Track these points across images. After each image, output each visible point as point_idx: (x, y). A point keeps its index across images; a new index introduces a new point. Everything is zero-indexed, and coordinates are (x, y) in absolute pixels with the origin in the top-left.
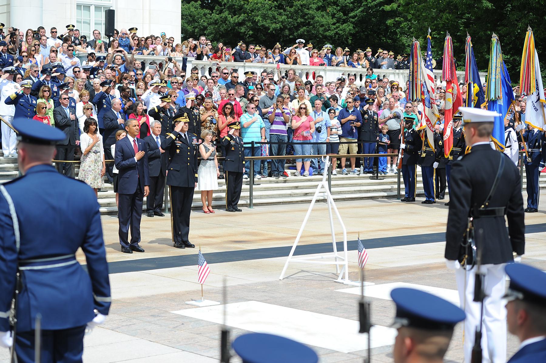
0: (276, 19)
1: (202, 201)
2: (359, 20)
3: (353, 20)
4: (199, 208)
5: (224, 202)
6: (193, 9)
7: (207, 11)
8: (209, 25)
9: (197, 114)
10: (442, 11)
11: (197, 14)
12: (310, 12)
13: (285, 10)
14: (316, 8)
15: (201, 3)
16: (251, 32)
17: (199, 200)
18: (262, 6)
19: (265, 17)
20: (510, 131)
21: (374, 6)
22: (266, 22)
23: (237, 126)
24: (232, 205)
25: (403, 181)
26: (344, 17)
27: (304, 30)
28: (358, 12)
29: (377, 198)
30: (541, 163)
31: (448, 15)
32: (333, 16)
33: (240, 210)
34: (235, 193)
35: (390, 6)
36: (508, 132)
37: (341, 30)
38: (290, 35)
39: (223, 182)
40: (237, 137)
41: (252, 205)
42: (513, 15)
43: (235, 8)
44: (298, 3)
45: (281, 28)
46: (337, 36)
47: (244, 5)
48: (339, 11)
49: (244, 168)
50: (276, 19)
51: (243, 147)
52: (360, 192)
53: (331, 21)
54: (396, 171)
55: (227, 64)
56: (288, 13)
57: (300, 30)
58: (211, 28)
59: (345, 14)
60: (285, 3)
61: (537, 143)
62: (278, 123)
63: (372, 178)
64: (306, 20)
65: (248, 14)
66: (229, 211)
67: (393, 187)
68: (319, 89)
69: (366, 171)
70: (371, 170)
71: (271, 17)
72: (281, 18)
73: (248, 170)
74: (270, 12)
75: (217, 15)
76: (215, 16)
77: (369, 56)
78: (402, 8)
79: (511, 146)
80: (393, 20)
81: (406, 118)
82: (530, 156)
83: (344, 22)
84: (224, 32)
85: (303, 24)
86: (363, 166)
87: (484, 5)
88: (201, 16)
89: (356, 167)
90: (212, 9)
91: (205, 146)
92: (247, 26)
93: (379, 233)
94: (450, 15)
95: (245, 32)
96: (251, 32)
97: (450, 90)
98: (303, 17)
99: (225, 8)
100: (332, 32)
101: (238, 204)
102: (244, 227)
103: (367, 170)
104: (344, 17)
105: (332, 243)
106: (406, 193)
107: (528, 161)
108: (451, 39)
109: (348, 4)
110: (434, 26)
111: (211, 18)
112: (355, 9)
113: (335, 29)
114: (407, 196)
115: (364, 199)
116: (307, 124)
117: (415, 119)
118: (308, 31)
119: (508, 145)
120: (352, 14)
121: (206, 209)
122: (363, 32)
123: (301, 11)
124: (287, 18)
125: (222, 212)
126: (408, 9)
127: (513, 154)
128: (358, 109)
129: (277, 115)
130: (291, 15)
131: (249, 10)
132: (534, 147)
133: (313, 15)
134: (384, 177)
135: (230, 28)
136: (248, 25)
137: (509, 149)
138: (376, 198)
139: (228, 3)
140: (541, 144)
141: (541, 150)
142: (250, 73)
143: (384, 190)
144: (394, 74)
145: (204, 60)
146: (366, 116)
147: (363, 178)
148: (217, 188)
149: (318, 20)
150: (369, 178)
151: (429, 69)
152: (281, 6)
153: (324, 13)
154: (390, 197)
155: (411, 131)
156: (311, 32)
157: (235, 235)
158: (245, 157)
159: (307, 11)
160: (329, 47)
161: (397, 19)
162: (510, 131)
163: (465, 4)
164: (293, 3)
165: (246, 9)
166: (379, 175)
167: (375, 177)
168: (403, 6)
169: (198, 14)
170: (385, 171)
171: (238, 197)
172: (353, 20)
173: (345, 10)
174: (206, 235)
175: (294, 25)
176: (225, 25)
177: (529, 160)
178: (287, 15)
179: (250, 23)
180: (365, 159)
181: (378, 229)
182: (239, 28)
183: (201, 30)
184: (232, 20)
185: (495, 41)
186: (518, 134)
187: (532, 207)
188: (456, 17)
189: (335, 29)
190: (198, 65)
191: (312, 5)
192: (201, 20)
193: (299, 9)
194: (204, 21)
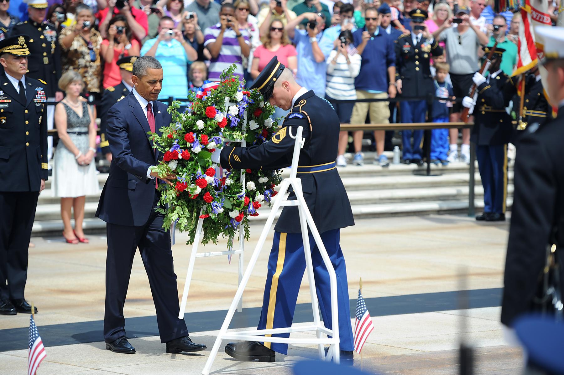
1: (63, 218)
62: (226, 59)
63: (417, 173)
69: (409, 159)
70: (417, 156)
81: (487, 49)
86: (400, 149)
105: (311, 304)
106: (486, 203)
115: (400, 215)
134: (442, 172)
166: (432, 166)
167: (423, 170)
180: (404, 134)
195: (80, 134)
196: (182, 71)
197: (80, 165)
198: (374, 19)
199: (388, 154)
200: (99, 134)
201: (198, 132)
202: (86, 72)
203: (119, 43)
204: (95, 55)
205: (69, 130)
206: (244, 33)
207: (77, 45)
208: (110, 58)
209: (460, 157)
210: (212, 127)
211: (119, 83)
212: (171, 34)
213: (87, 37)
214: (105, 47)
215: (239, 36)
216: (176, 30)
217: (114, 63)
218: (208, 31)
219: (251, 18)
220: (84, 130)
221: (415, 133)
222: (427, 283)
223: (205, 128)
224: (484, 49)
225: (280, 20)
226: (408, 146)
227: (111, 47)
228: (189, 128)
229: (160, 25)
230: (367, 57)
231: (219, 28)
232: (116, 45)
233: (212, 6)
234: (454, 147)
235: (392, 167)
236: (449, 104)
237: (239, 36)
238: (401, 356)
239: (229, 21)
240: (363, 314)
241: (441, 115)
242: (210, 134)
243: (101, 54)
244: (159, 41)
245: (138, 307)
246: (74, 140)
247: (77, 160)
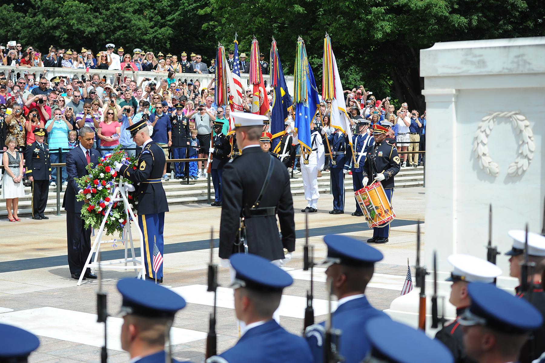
0: (91, 23)
1: (7, 210)
2: (177, 23)
3: (171, 23)
4: (5, 217)
5: (30, 210)
6: (5, 12)
7: (20, 14)
8: (23, 28)
9: (2, 121)
10: (255, 15)
11: (10, 17)
12: (127, 15)
13: (101, 14)
14: (132, 12)
15: (13, 6)
16: (66, 36)
17: (4, 209)
18: (77, 9)
19: (80, 20)
20: (316, 135)
21: (191, 10)
22: (82, 25)
23: (41, 132)
24: (38, 212)
25: (213, 185)
26: (162, 21)
27: (121, 34)
28: (176, 15)
29: (188, 203)
30: (345, 165)
31: (260, 19)
32: (151, 19)
33: (48, 218)
34: (41, 200)
35: (204, 10)
36: (314, 136)
37: (160, 34)
38: (106, 39)
39: (29, 189)
40: (42, 144)
41: (59, 212)
42: (324, 19)
43: (49, 11)
44: (113, 6)
45: (96, 31)
46: (155, 40)
47: (58, 8)
48: (157, 14)
49: (50, 176)
50: (91, 23)
51: (48, 154)
52: (171, 197)
53: (148, 24)
54: (207, 176)
55: (36, 69)
56: (104, 16)
57: (116, 33)
58: (24, 32)
59: (163, 18)
60: (100, 6)
61: (342, 146)
63: (182, 183)
64: (122, 23)
65: (62, 17)
66: (36, 219)
67: (204, 191)
68: (127, 94)
69: (178, 176)
70: (182, 175)
71: (87, 20)
72: (97, 21)
73: (55, 177)
74: (85, 15)
75: (31, 19)
76: (29, 19)
77: (184, 60)
78: (215, 12)
79: (317, 149)
80: (207, 24)
81: (215, 123)
82: (334, 159)
83: (162, 26)
84: (38, 36)
85: (120, 28)
86: (174, 172)
87: (296, 9)
88: (14, 19)
89: (167, 172)
90: (25, 12)
91: (9, 154)
92: (62, 30)
93: (184, 237)
94: (263, 19)
95: (60, 36)
96: (66, 36)
97: (257, 93)
98: (119, 20)
99: (38, 11)
100: (151, 36)
101: (44, 212)
102: (49, 235)
103: (178, 175)
104: (162, 21)
107: (333, 164)
108: (257, 43)
109: (165, 7)
110: (248, 30)
111: (24, 22)
112: (173, 13)
113: (153, 32)
114: (218, 201)
115: (174, 204)
116: (112, 129)
117: (224, 123)
118: (124, 35)
119: (314, 148)
120: (169, 18)
121: (12, 218)
122: (182, 35)
123: (117, 15)
124: (103, 21)
125: (28, 220)
126: (222, 13)
127: (320, 157)
128: (167, 114)
129: (88, 121)
130: (107, 19)
131: (64, 13)
132: (339, 150)
133: (129, 18)
134: (195, 182)
135: (45, 32)
136: (63, 29)
137: (315, 151)
138: (187, 203)
139: (42, 6)
140: (345, 147)
141: (345, 153)
142: (58, 78)
143: (194, 195)
144: (207, 78)
145: (12, 64)
146: (175, 121)
147: (174, 184)
148: (24, 196)
149: (135, 23)
150: (179, 183)
151: (236, 74)
152: (96, 10)
153: (141, 17)
154: (200, 202)
155: (220, 136)
156: (127, 35)
157: (38, 243)
158: (51, 164)
159: (124, 14)
160: (138, 51)
161: (211, 23)
162: (316, 135)
163: (278, 9)
164: (109, 6)
165: (61, 12)
166: (190, 180)
167: (185, 182)
168: (217, 10)
169: (11, 17)
170: (195, 175)
171: (45, 205)
172: (171, 23)
173: (163, 14)
174: (9, 244)
175: (110, 28)
176: (40, 28)
177: (334, 163)
178: (103, 18)
179: (65, 27)
180: (175, 164)
181: (183, 234)
182: (53, 32)
183: (14, 33)
184: (46, 24)
185: (300, 44)
186: (323, 137)
187: (338, 208)
188: (269, 22)
189: (153, 32)
190: (6, 71)
191: (129, 8)
192: (14, 24)
193: (115, 12)
194: (17, 25)
195: (15, 167)
196: (65, 135)
197: (15, 182)
198: (160, 108)
199: (169, 174)
200: (24, 167)
201: (102, 179)
202: (18, 136)
203: (34, 122)
204: (22, 128)
205: (9, 166)
206: (96, 116)
207: (13, 122)
208: (30, 129)
209: (203, 175)
210: (108, 177)
211: (33, 141)
212: (60, 117)
213: (18, 119)
214: (27, 124)
215: (93, 118)
216: (62, 115)
217: (32, 132)
218: (78, 115)
219: (100, 109)
220: (17, 165)
221: (181, 164)
222: (188, 237)
223: (105, 177)
224: (213, 123)
225: (112, 110)
226: (177, 170)
227: (30, 124)
228: (96, 177)
229: (54, 113)
230: (157, 128)
231: (83, 114)
232: (32, 123)
233: (80, 103)
234: (200, 170)
235: (170, 180)
236: (197, 149)
237: (93, 118)
238: (176, 273)
239: (88, 110)
240: (157, 253)
241: (194, 155)
242: (107, 180)
243: (25, 127)
244: (54, 121)
245: (45, 252)
246: (12, 170)
247: (13, 180)
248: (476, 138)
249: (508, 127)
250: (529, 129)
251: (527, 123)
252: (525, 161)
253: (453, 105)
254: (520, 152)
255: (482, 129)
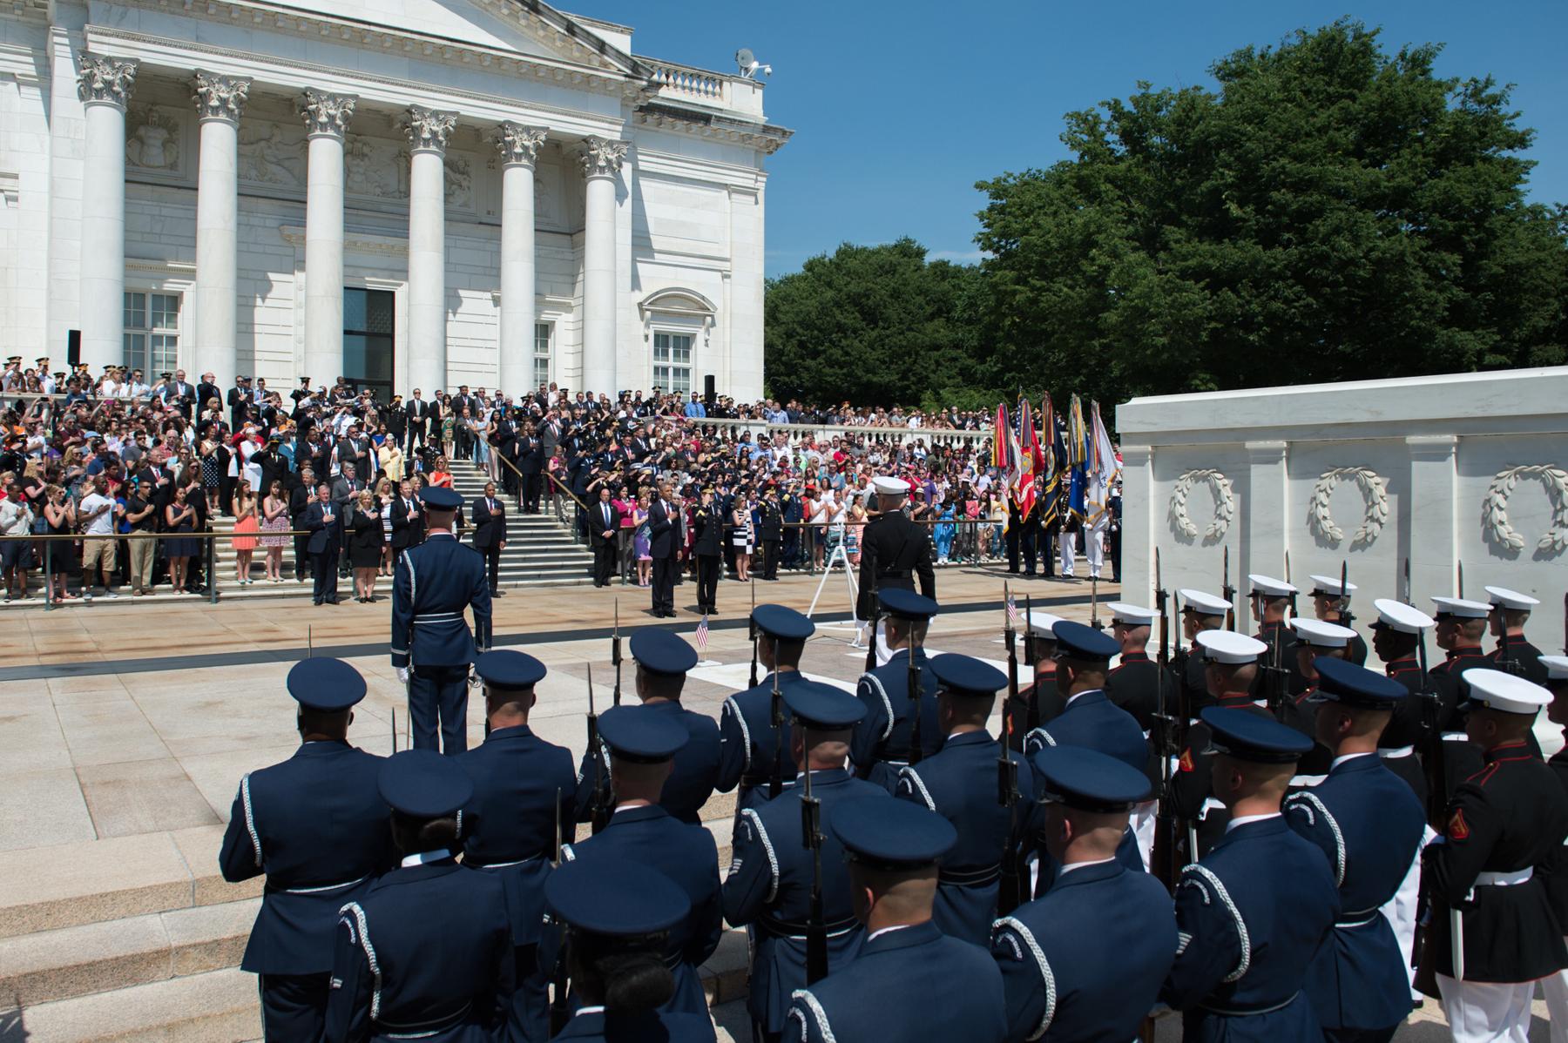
248: (1488, 501)
249: (1206, 485)
250: (1228, 488)
251: (1226, 481)
252: (1376, 525)
253: (1284, 463)
254: (1370, 514)
255: (1322, 488)
